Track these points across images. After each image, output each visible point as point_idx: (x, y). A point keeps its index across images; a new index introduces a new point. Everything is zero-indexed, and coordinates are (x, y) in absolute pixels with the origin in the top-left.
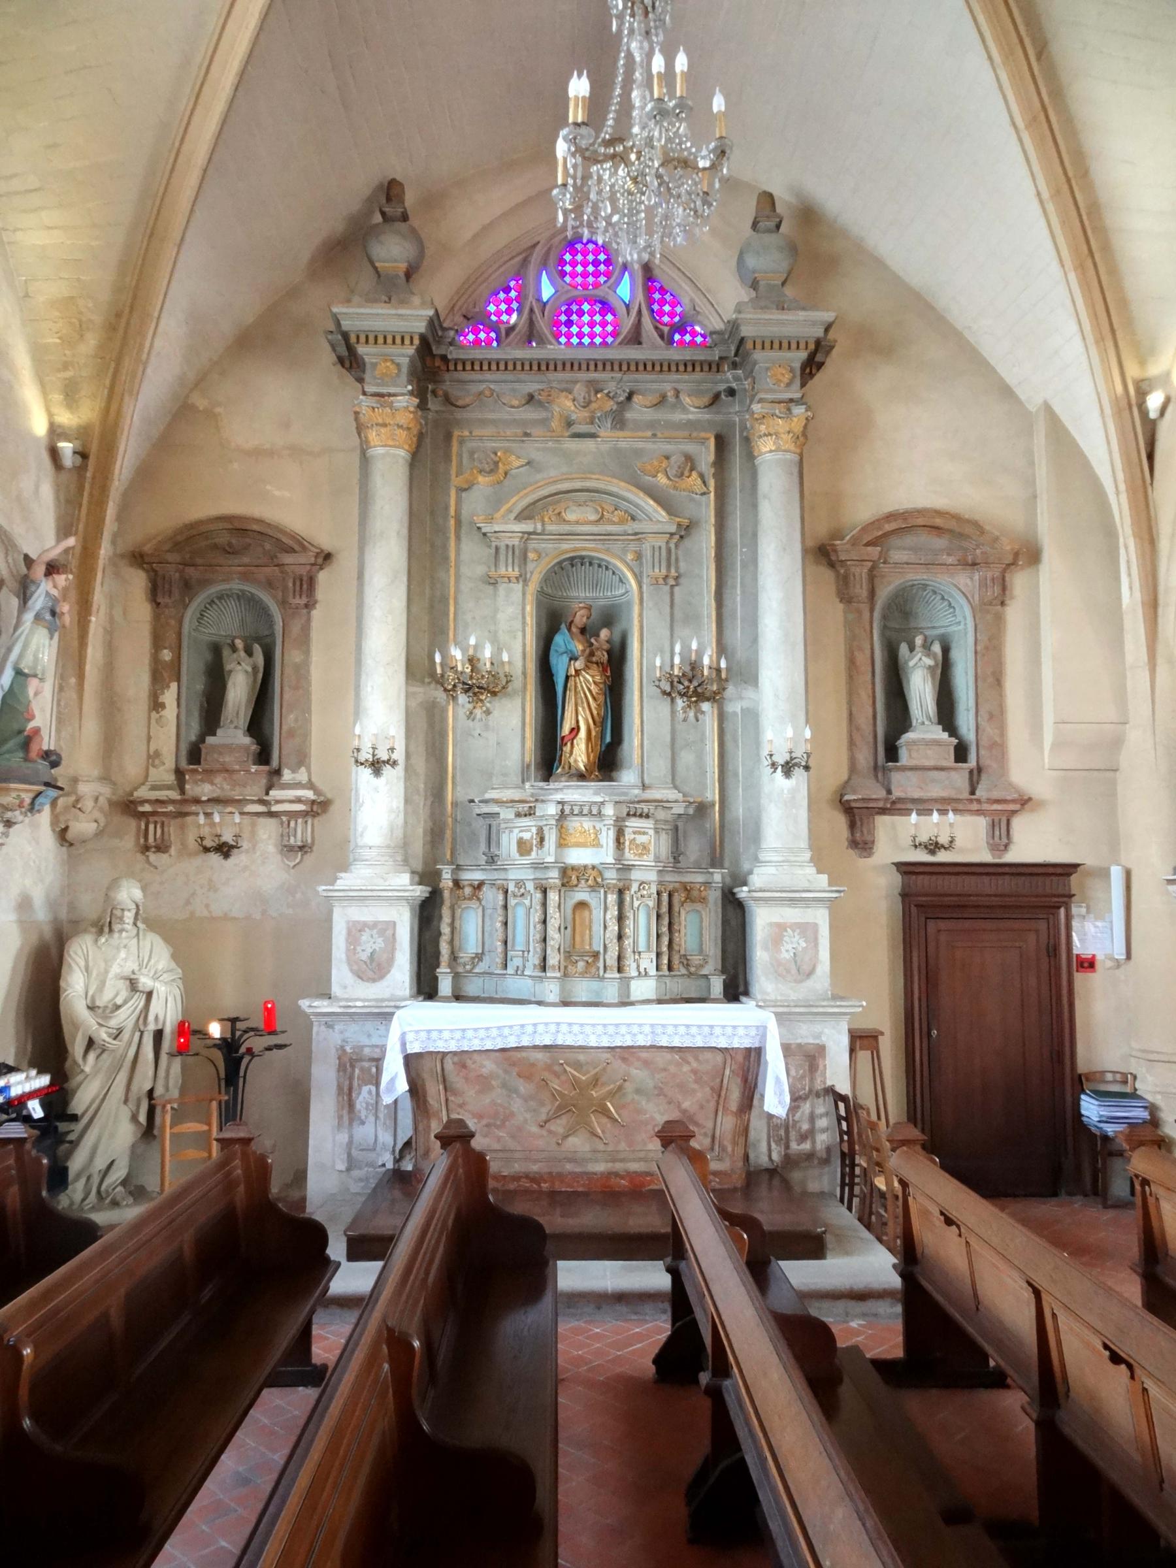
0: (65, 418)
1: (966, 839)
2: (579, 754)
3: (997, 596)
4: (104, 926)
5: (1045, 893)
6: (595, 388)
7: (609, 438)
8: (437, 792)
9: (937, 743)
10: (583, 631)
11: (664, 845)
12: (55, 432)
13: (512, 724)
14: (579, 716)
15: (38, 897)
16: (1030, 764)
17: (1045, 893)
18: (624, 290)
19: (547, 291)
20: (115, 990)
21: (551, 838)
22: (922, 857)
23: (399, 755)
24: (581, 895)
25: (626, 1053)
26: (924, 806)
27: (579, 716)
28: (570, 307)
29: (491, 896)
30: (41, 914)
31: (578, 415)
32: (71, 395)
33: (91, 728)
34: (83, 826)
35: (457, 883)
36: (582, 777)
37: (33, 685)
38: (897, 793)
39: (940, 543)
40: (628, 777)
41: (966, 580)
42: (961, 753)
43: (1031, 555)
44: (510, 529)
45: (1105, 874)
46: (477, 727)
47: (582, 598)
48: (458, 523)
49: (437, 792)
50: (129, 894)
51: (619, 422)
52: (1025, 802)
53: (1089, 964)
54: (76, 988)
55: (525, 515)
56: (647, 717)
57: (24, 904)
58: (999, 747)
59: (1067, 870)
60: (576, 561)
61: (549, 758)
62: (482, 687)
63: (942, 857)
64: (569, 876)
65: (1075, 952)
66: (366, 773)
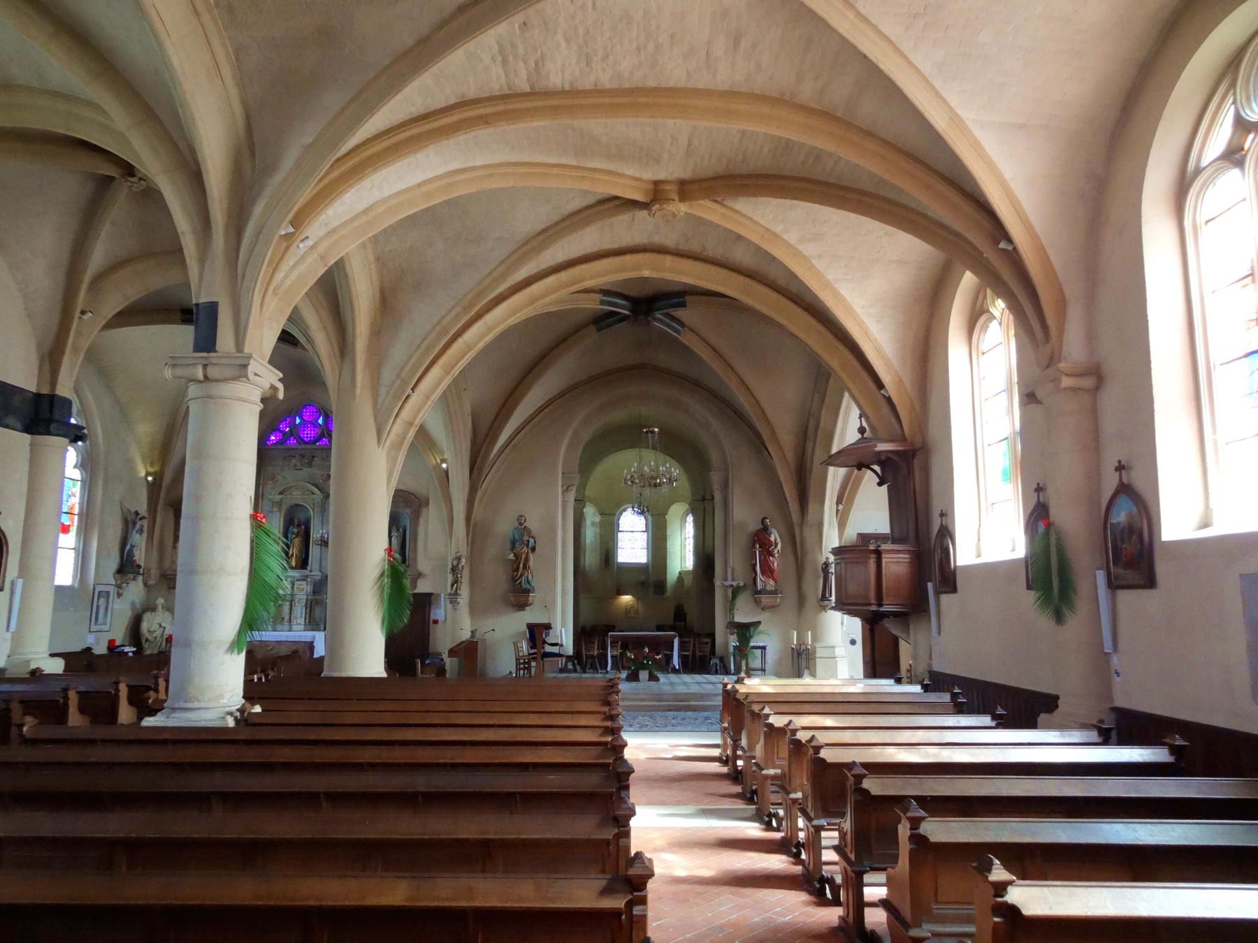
0: (151, 470)
3: (416, 515)
4: (153, 609)
6: (303, 456)
7: (306, 471)
10: (299, 526)
11: (309, 589)
12: (148, 474)
15: (138, 601)
16: (423, 564)
18: (320, 421)
19: (298, 421)
20: (155, 627)
25: (279, 642)
28: (304, 424)
30: (138, 606)
32: (152, 465)
33: (155, 555)
34: (151, 582)
41: (408, 511)
45: (439, 595)
47: (301, 516)
50: (160, 601)
51: (310, 465)
52: (420, 575)
53: (436, 622)
54: (145, 626)
56: (314, 551)
57: (133, 604)
58: (415, 560)
60: (297, 505)
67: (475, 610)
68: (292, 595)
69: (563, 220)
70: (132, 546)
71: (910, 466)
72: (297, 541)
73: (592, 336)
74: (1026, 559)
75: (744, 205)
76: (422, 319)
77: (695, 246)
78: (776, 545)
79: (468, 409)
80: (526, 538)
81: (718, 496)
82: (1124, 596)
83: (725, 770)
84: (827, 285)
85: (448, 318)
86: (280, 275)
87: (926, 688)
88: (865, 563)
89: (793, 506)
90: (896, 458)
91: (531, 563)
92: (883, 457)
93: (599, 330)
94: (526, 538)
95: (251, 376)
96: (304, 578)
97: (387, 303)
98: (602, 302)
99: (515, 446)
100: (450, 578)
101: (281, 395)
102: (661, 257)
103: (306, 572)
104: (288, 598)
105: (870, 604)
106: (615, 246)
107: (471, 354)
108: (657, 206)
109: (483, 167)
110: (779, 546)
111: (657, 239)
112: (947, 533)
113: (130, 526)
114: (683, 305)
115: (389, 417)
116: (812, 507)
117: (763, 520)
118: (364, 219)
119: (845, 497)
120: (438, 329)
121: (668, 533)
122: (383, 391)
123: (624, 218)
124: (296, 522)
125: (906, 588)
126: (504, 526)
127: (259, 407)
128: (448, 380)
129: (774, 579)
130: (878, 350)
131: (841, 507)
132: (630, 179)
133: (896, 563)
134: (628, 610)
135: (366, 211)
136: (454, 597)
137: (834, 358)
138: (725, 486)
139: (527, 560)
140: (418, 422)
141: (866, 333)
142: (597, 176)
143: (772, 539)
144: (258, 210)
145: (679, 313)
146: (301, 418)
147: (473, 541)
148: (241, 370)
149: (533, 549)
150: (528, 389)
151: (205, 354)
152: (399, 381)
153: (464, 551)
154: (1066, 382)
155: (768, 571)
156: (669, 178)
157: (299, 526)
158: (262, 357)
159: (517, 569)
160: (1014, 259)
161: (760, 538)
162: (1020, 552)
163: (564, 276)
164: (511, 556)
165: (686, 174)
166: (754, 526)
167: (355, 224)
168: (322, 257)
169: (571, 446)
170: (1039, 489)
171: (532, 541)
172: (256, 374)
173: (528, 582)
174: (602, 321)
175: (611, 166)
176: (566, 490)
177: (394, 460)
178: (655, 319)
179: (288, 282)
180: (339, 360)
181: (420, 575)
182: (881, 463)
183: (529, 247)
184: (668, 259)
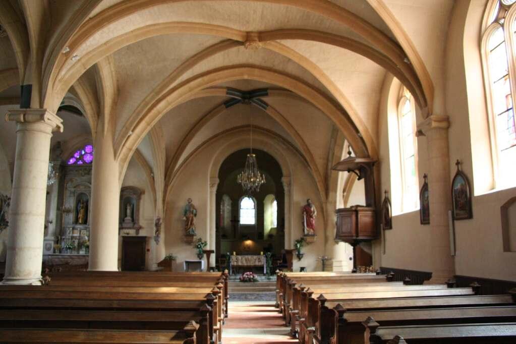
1: (132, 233)
2: (80, 221)
3: (139, 198)
5: (143, 241)
6: (86, 169)
8: (61, 226)
9: (129, 220)
13: (71, 217)
14: (80, 215)
16: (142, 222)
17: (143, 241)
19: (83, 153)
21: (71, 232)
22: (126, 235)
23: (54, 221)
24: (74, 240)
26: (125, 228)
27: (80, 215)
29: (65, 240)
31: (83, 173)
35: (61, 238)
36: (80, 224)
37: (5, 213)
38: (123, 226)
39: (131, 191)
40: (88, 224)
41: (135, 196)
42: (133, 220)
43: (143, 192)
44: (73, 190)
46: (67, 217)
48: (66, 188)
49: (61, 226)
52: (140, 228)
55: (75, 187)
58: (138, 220)
59: (145, 238)
61: (76, 221)
62: (68, 211)
63: (129, 235)
64: (72, 237)
65: (146, 248)
66: (49, 224)
67: (168, 244)
68: (79, 236)
69: (204, 50)
70: (4, 212)
71: (371, 170)
72: (82, 211)
73: (225, 112)
74: (420, 209)
75: (289, 43)
76: (137, 98)
77: (269, 65)
78: (314, 212)
79: (163, 146)
80: (192, 210)
81: (286, 188)
82: (457, 223)
83: (281, 315)
84: (331, 83)
85: (148, 98)
86: (63, 73)
87: (378, 274)
88: (351, 217)
89: (322, 194)
90: (365, 166)
91: (194, 221)
92: (359, 165)
93: (227, 107)
94: (192, 210)
95: (46, 119)
96: (86, 229)
97: (121, 92)
98: (227, 93)
100: (155, 229)
101: (62, 130)
102: (253, 69)
103: (87, 226)
104: (78, 238)
105: (352, 236)
106: (231, 64)
107: (160, 116)
108: (248, 43)
109: (163, 23)
110: (316, 213)
111: (251, 61)
112: (388, 201)
113: (3, 203)
114: (266, 95)
115: (119, 146)
116: (331, 194)
117: (308, 201)
118: (104, 47)
119: (347, 189)
120: (144, 103)
121: (265, 209)
122: (117, 133)
123: (234, 50)
124: (82, 201)
125: (370, 230)
126: (182, 204)
127: (50, 136)
128: (149, 128)
129: (313, 229)
130: (356, 114)
131: (345, 194)
132: (235, 29)
133: (365, 218)
135: (105, 44)
136: (157, 239)
137: (336, 119)
138: (290, 185)
140: (134, 148)
141: (350, 106)
142: (219, 29)
143: (312, 209)
144: (52, 42)
145: (265, 99)
146: (85, 151)
147: (166, 210)
148: (42, 117)
149: (195, 215)
150: (193, 135)
151: (25, 109)
152: (124, 129)
153: (162, 215)
154: (434, 124)
155: (310, 225)
156: (254, 30)
157: (83, 203)
158: (54, 112)
159: (187, 225)
160: (410, 67)
161: (307, 210)
162: (418, 208)
163: (206, 78)
164: (185, 218)
165: (262, 28)
166: (303, 204)
167: (101, 49)
168: (84, 65)
169: (214, 165)
170: (425, 177)
171: (194, 211)
172: (48, 119)
173: (193, 231)
174: (228, 103)
175: (225, 24)
176: (212, 186)
177: (122, 168)
178: (255, 102)
179: (67, 76)
180: (96, 118)
181: (140, 228)
182: (360, 170)
183: (187, 63)
184: (257, 71)
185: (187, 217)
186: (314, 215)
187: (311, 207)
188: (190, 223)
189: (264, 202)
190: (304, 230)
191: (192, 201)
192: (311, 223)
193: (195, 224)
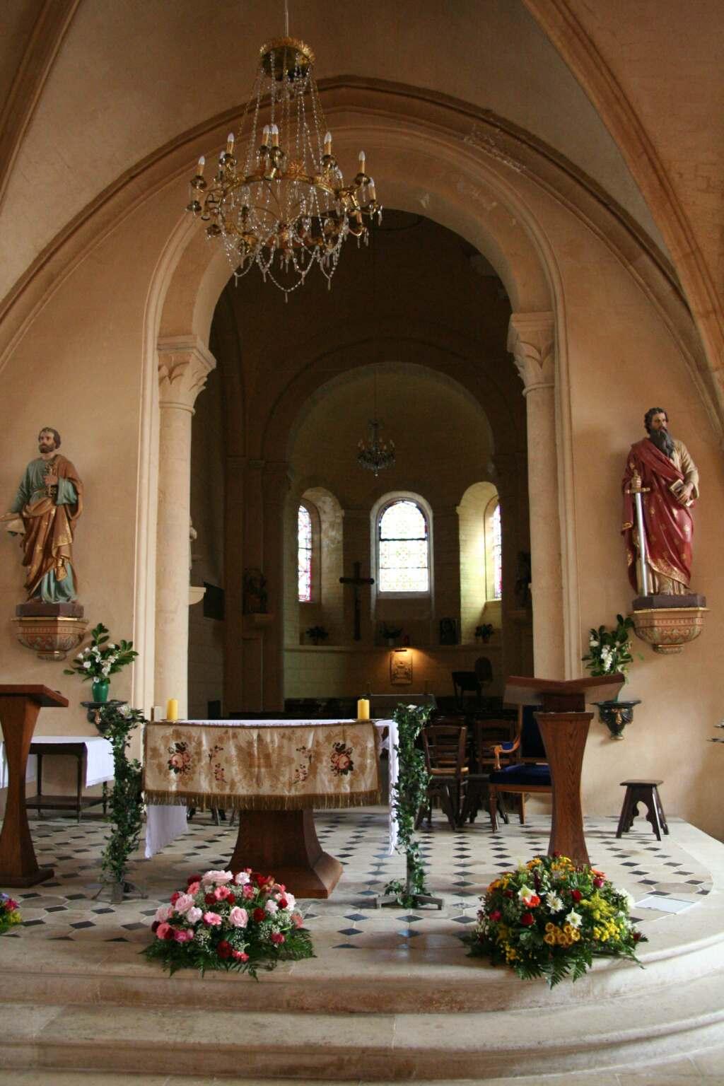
78: (687, 478)
80: (51, 480)
81: (531, 373)
91: (63, 541)
94: (51, 480)
99: (50, 281)
110: (696, 479)
117: (648, 418)
121: (462, 537)
134: (408, 672)
138: (550, 351)
139: (53, 533)
143: (676, 461)
149: (73, 508)
155: (668, 545)
159: (28, 561)
161: (647, 466)
164: (16, 525)
166: (625, 437)
169: (184, 279)
171: (65, 487)
173: (60, 589)
176: (170, 374)
185: (25, 521)
186: (687, 492)
187: (669, 451)
188: (39, 548)
189: (459, 510)
190: (633, 573)
191: (57, 441)
192: (671, 534)
193: (65, 553)
